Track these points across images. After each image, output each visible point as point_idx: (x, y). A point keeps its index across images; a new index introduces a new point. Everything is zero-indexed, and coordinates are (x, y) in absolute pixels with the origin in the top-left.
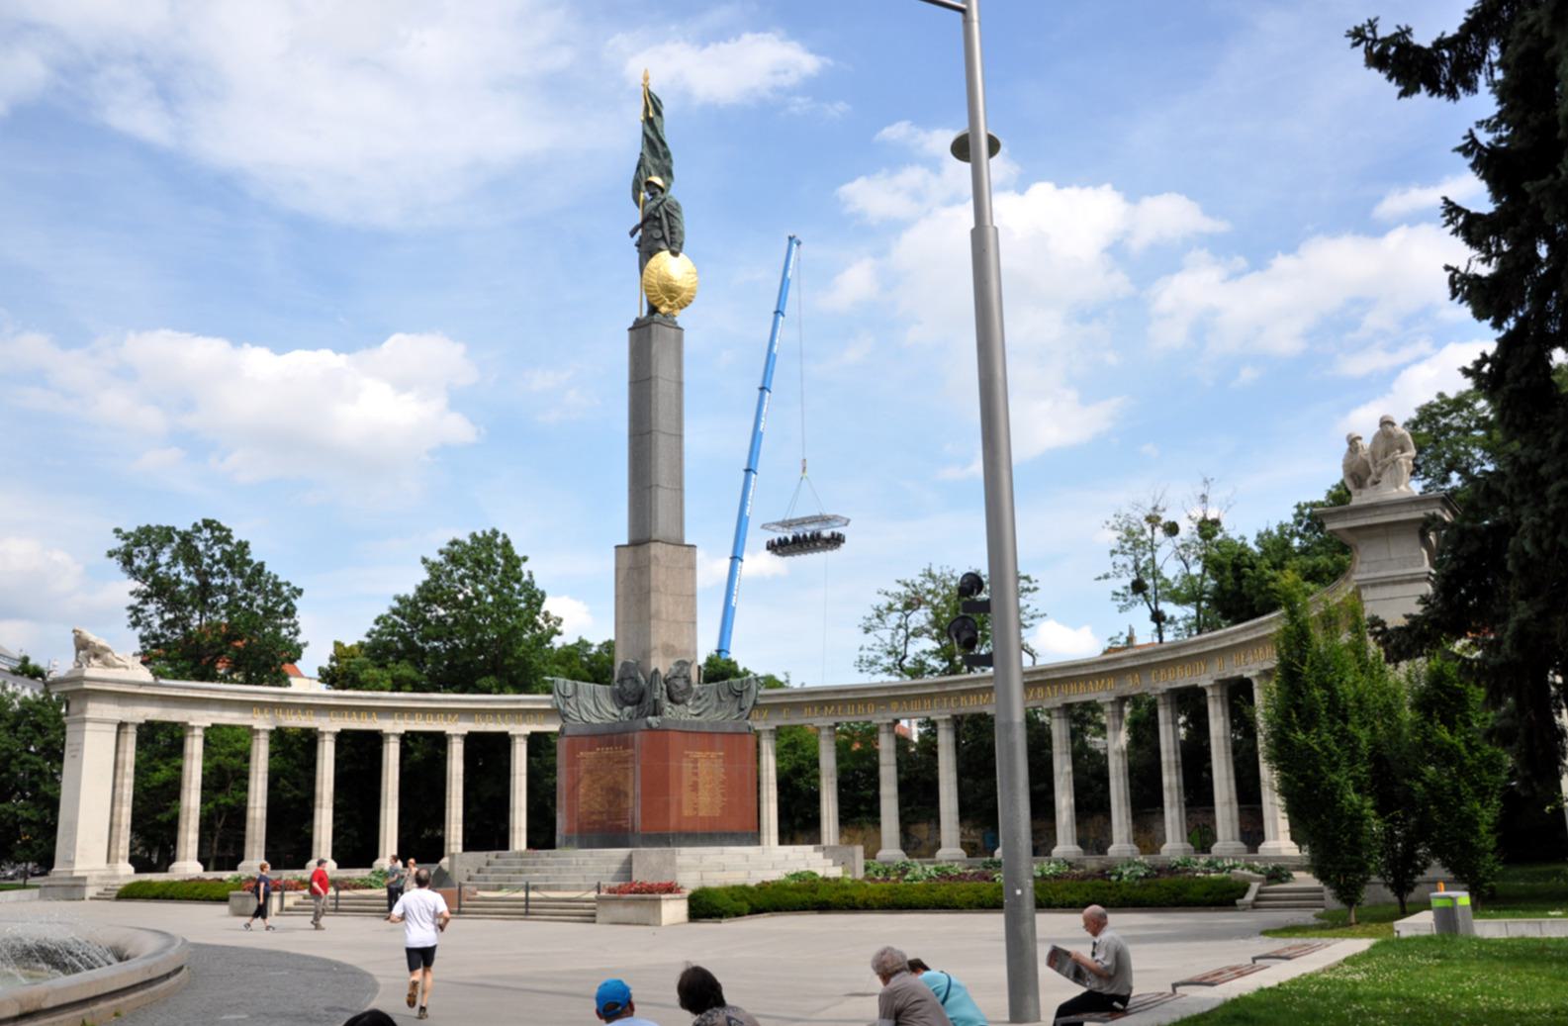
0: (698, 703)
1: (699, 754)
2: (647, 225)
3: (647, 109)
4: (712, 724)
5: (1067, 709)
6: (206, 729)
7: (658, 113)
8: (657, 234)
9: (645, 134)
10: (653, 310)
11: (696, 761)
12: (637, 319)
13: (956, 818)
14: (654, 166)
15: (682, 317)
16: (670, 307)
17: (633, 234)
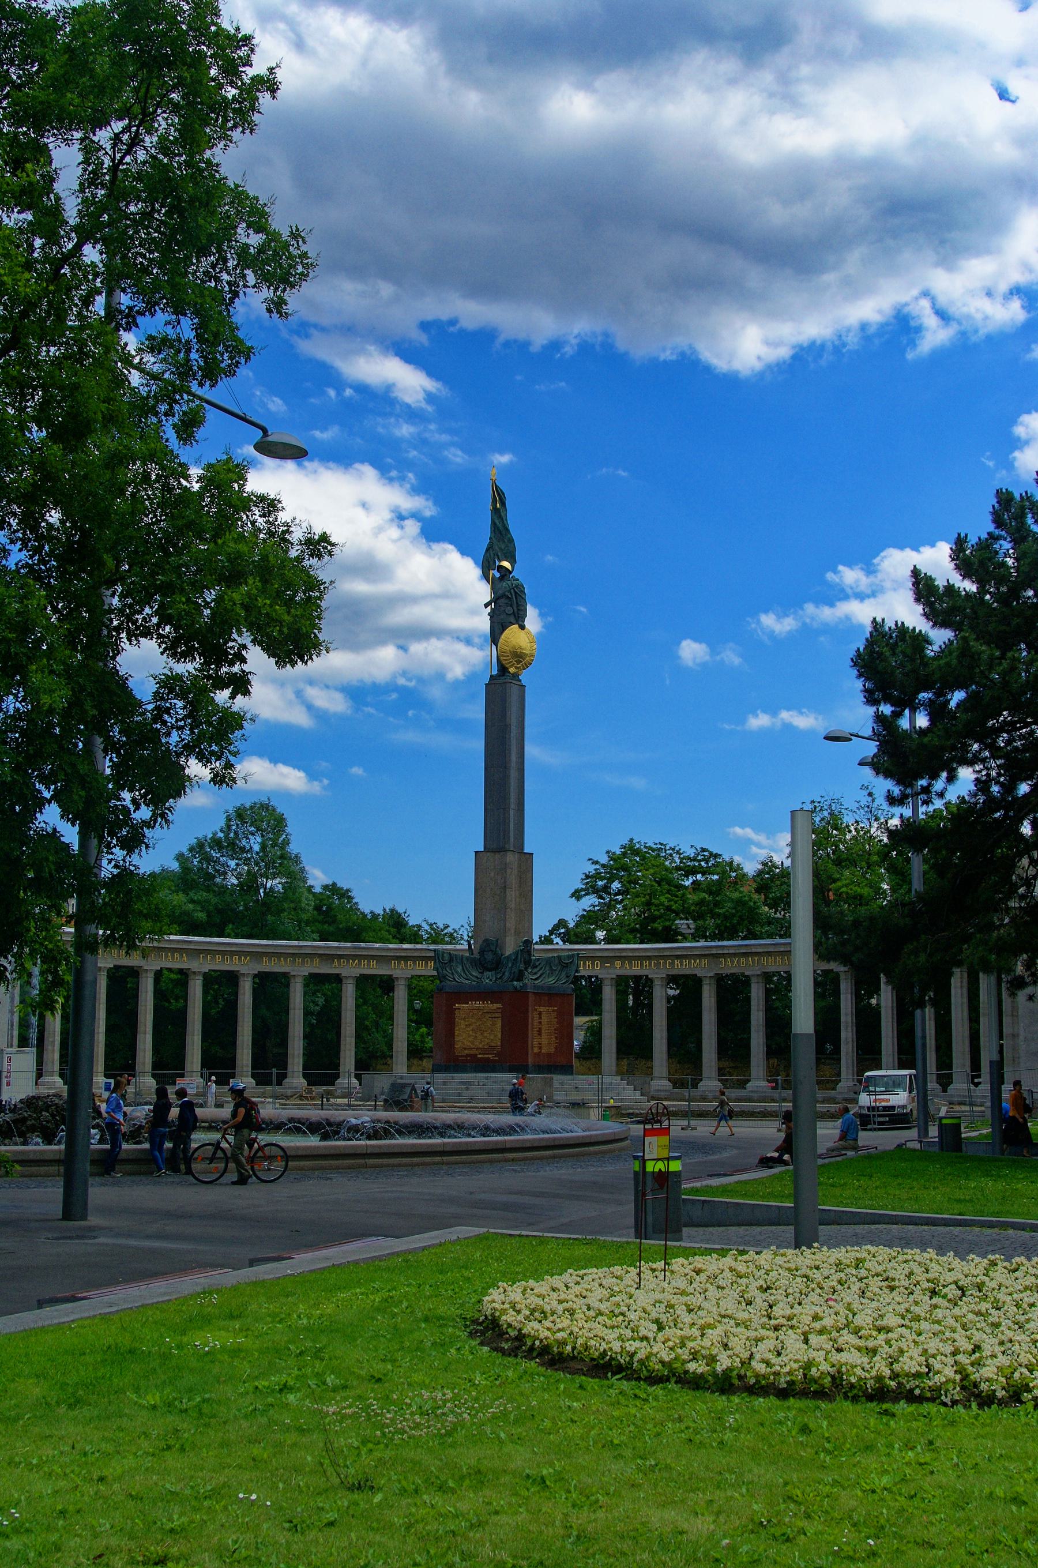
0: (535, 970)
1: (542, 1009)
2: (502, 601)
3: (494, 501)
4: (549, 988)
5: (767, 977)
6: (109, 970)
7: (503, 504)
8: (509, 610)
9: (493, 524)
10: (503, 669)
11: (540, 1013)
12: (492, 676)
13: (665, 1056)
14: (501, 549)
15: (525, 677)
16: (517, 668)
17: (486, 606)
